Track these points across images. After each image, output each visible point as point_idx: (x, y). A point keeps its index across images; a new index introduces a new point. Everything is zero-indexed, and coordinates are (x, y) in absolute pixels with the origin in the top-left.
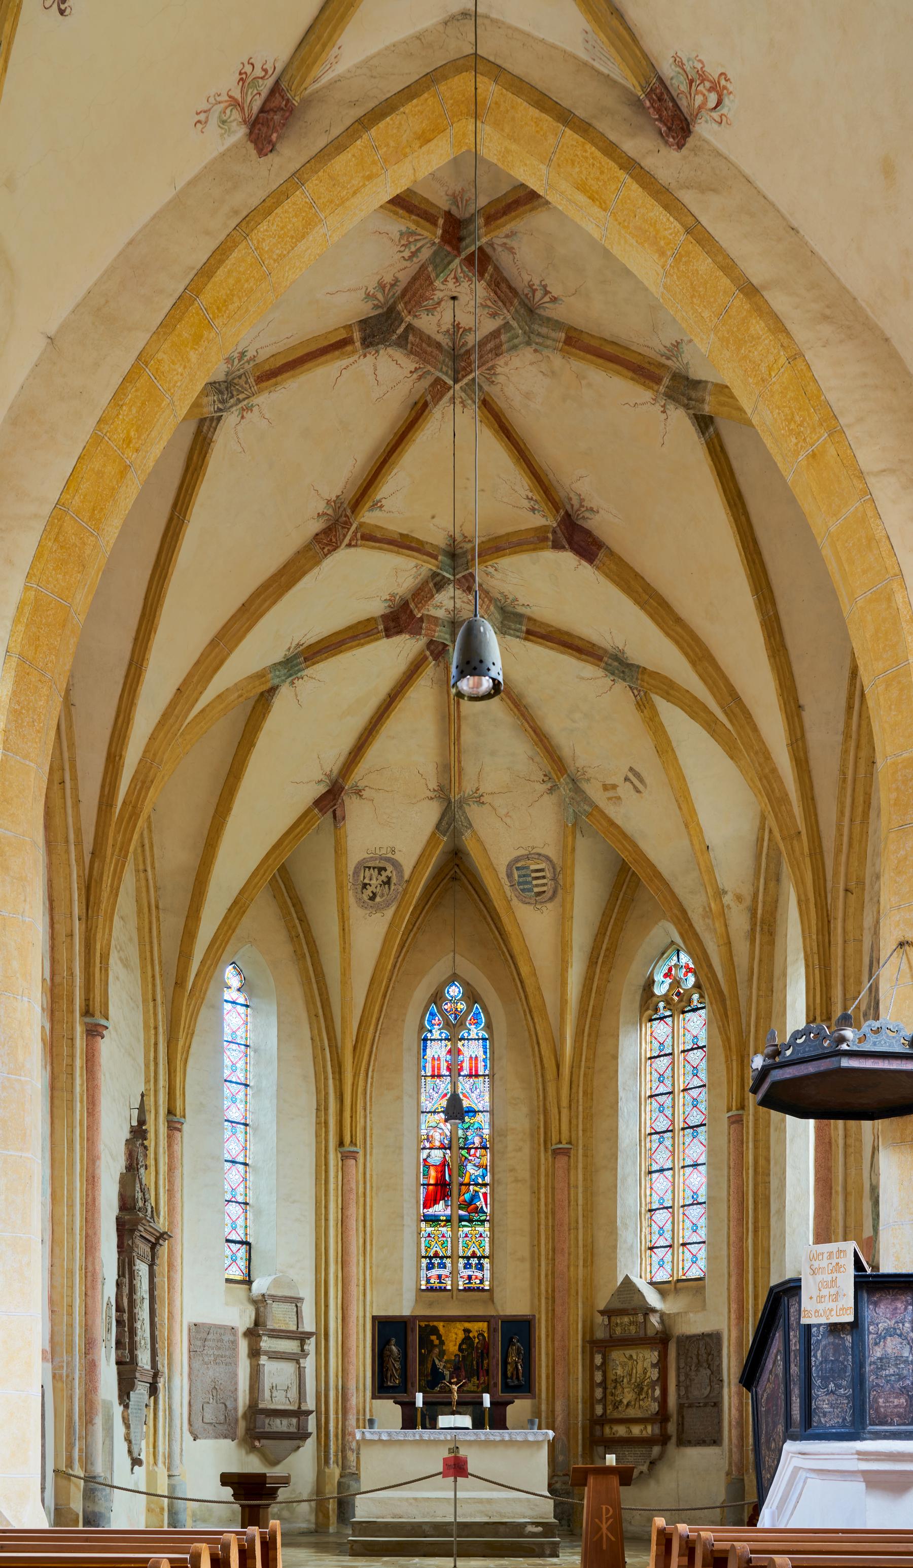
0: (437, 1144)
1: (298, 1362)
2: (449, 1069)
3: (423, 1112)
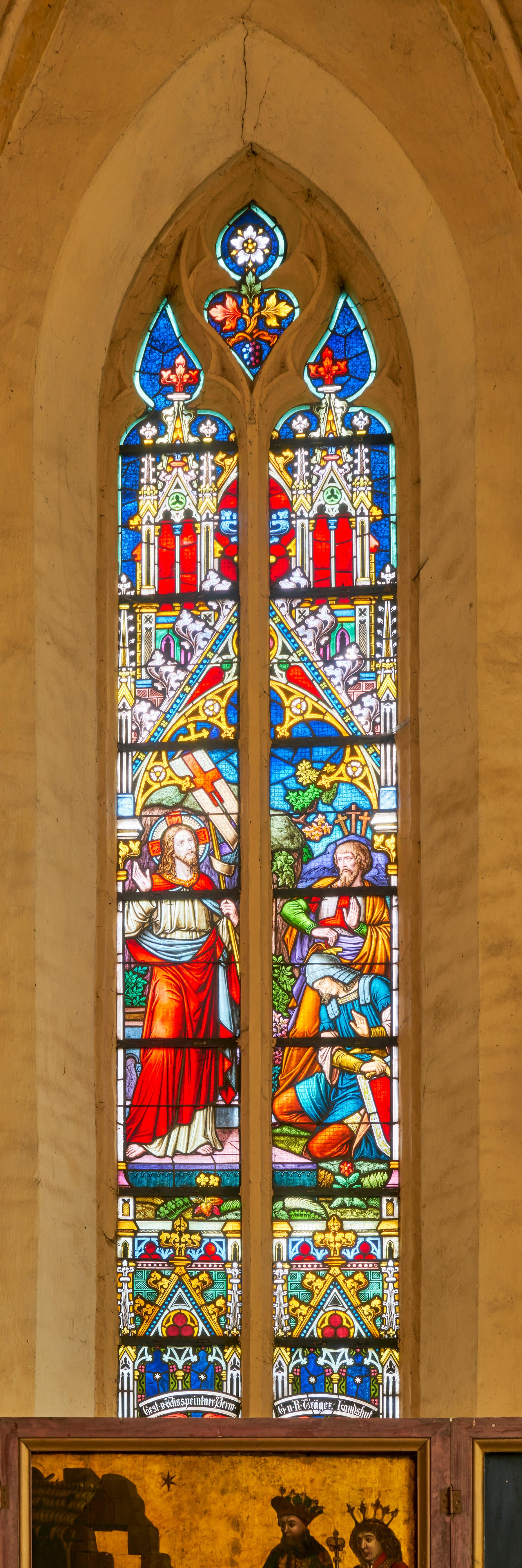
0: (184, 875)
2: (228, 569)
3: (123, 748)
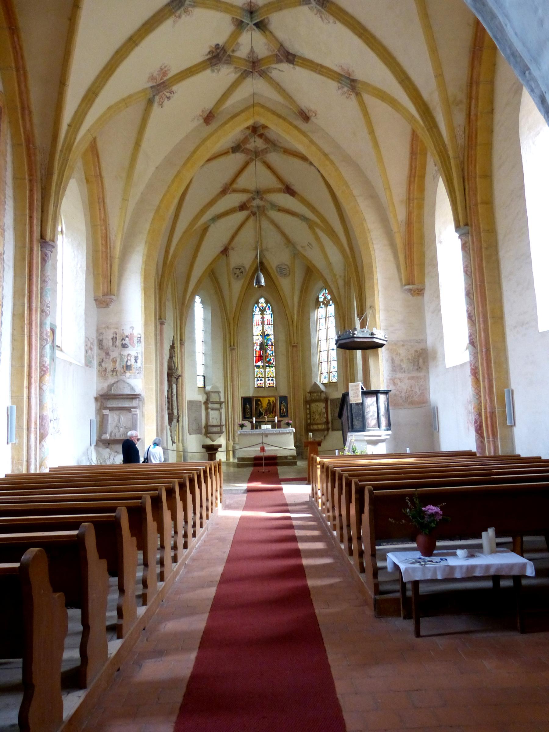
1: (220, 410)
